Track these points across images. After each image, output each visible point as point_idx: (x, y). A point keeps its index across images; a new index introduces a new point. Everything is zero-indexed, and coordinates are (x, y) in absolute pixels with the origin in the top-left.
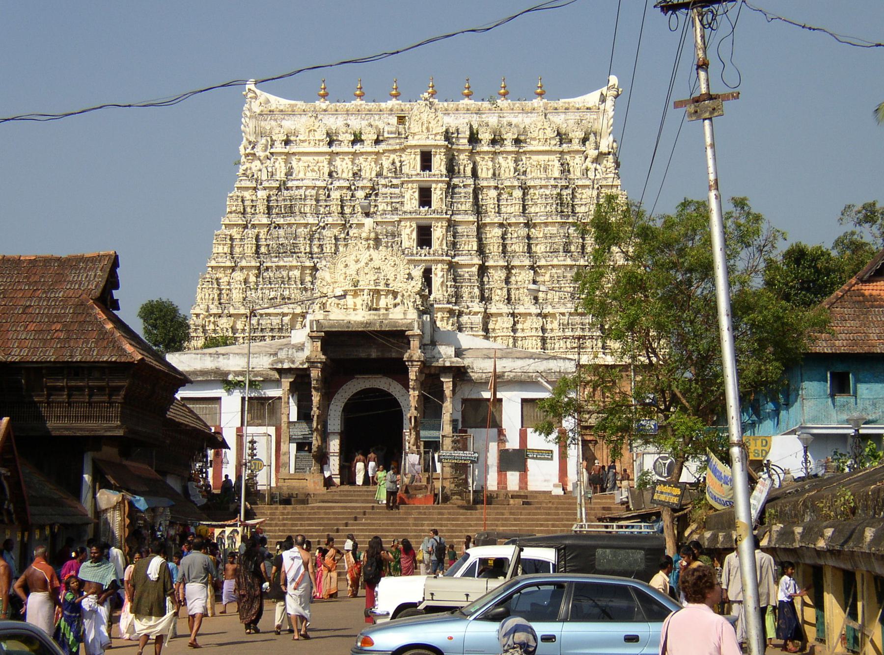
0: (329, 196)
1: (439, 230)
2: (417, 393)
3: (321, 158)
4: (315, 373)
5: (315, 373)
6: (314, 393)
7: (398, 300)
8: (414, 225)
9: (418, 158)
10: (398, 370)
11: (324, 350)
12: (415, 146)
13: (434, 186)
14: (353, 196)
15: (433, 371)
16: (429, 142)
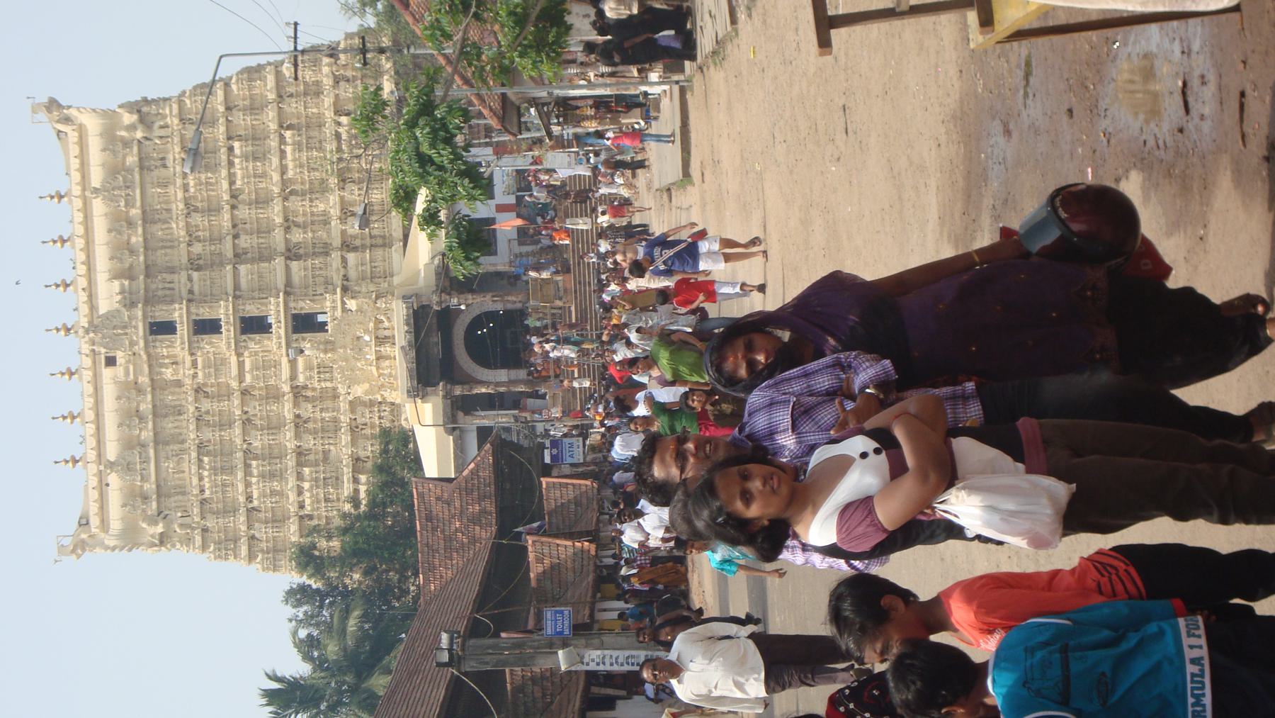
0: (209, 441)
1: (248, 308)
2: (470, 296)
3: (163, 454)
4: (458, 391)
5: (458, 391)
6: (475, 391)
7: (382, 318)
8: (244, 337)
9: (160, 337)
10: (446, 317)
11: (435, 385)
12: (146, 342)
13: (194, 317)
14: (207, 412)
15: (447, 284)
16: (140, 325)
